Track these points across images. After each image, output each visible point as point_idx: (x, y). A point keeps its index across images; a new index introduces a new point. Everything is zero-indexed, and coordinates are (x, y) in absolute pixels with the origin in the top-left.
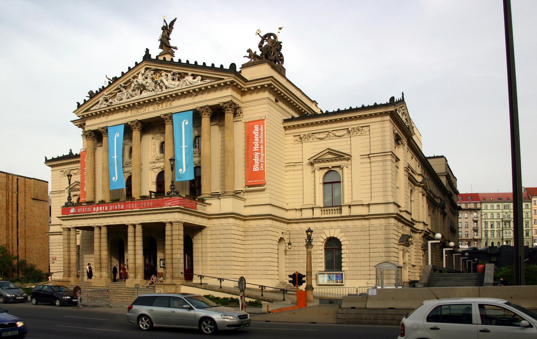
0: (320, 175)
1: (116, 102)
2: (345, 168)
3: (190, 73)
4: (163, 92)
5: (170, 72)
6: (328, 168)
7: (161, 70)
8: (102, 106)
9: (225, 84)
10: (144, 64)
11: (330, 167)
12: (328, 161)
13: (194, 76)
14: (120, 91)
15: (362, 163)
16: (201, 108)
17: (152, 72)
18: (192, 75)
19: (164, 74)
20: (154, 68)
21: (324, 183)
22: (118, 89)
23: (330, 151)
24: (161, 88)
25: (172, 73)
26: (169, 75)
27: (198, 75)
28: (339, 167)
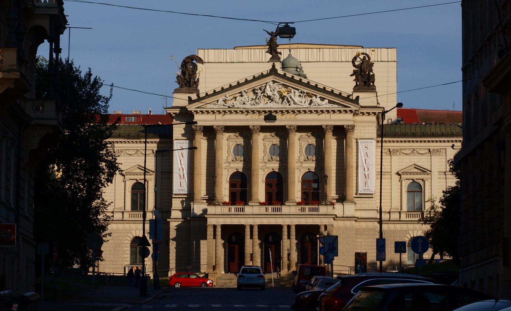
0: (406, 184)
1: (237, 104)
2: (427, 182)
3: (318, 96)
4: (291, 107)
5: (298, 90)
6: (413, 180)
7: (289, 86)
8: (220, 105)
9: (351, 111)
10: (272, 77)
11: (414, 179)
12: (414, 173)
13: (322, 99)
14: (242, 96)
15: (439, 178)
16: (327, 126)
17: (280, 86)
18: (320, 97)
19: (293, 90)
20: (282, 83)
21: (408, 191)
22: (241, 93)
23: (416, 167)
24: (289, 102)
25: (300, 91)
26: (296, 91)
27: (325, 99)
28: (423, 180)
